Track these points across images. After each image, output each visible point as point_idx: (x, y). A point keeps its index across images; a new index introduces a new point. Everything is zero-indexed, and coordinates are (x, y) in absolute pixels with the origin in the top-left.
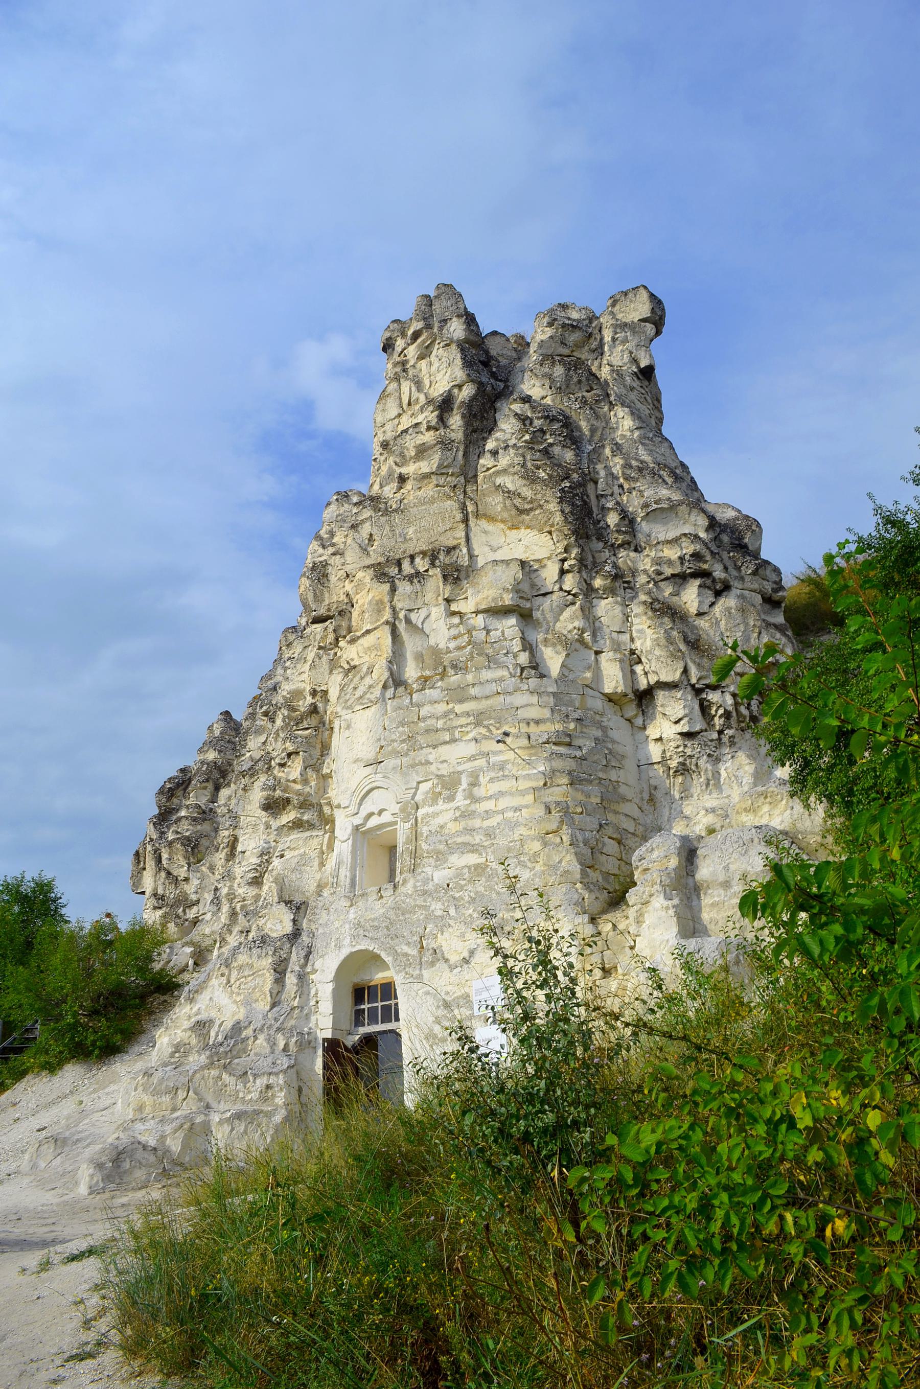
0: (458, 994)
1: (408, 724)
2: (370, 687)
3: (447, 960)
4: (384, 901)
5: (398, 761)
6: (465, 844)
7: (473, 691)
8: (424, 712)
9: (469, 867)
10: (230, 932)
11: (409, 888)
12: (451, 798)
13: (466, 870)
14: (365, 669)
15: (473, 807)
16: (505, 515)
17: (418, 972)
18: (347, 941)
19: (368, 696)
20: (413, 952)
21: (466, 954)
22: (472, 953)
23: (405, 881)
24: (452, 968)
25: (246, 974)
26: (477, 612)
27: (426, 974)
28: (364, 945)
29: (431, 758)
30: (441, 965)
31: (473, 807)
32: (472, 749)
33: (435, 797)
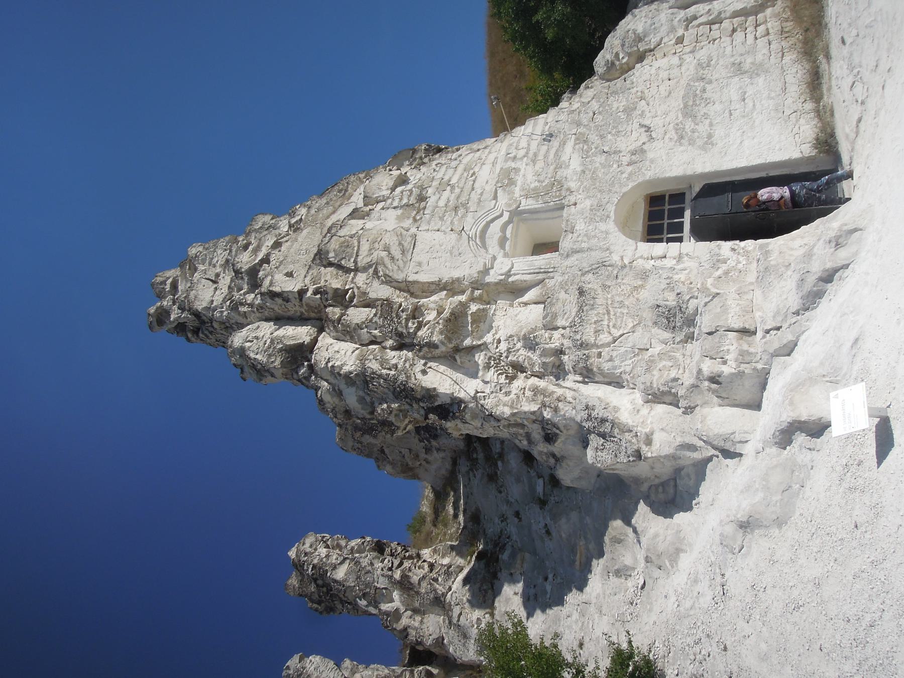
0: (673, 132)
1: (446, 211)
2: (400, 244)
3: (644, 143)
4: (578, 202)
5: (470, 215)
6: (557, 151)
7: (446, 178)
8: (442, 203)
9: (575, 144)
10: (553, 392)
11: (573, 185)
12: (517, 170)
13: (577, 146)
14: (384, 254)
15: (531, 154)
16: (338, 203)
17: (648, 163)
18: (602, 226)
19: (406, 244)
20: (630, 168)
21: (643, 129)
22: (642, 126)
23: (568, 189)
24: (651, 138)
25: (606, 323)
26: (393, 189)
27: (650, 155)
28: (611, 208)
29: (479, 191)
30: (645, 147)
31: (531, 154)
32: (487, 168)
33: (512, 183)
